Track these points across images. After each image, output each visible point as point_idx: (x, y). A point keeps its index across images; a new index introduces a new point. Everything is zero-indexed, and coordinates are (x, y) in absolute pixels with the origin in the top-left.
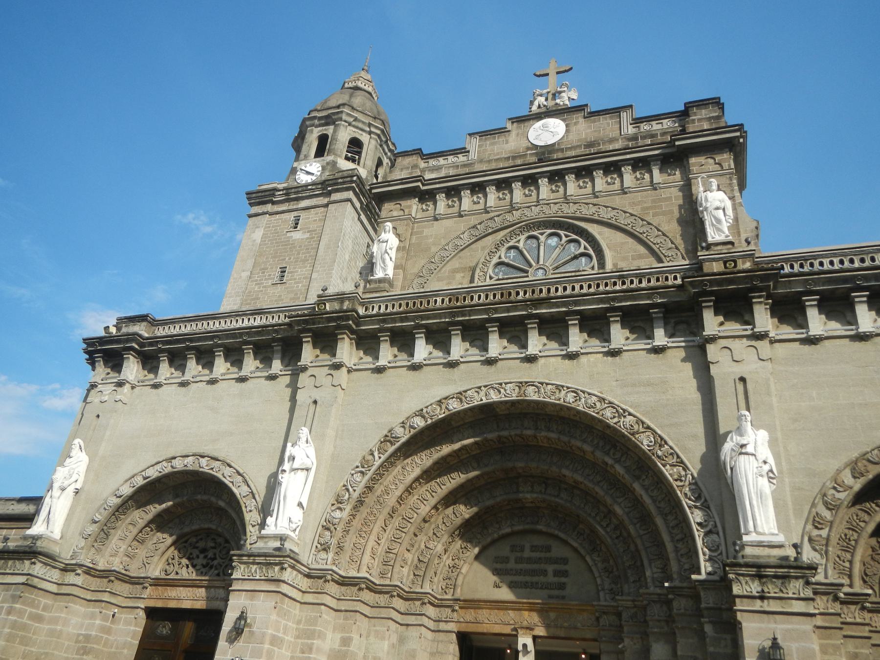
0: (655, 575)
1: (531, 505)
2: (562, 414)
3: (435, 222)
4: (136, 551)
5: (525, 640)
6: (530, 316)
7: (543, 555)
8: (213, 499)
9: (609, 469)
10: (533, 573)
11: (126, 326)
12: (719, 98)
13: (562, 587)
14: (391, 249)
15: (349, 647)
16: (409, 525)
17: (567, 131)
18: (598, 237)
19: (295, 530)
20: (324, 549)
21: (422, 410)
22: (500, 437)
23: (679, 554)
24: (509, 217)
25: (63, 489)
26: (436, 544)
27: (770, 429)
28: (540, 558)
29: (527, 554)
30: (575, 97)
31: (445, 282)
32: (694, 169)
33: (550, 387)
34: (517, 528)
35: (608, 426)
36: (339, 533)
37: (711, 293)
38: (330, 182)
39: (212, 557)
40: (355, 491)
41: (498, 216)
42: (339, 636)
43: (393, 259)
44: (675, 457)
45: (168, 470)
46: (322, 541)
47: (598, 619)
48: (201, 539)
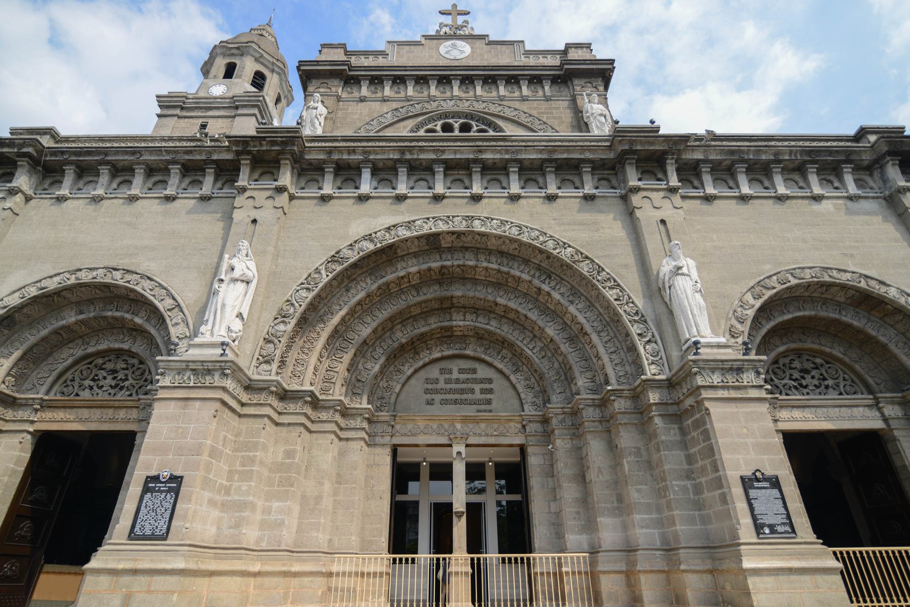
0: (586, 385)
1: (459, 333)
2: (504, 248)
4: (24, 371)
6: (476, 161)
7: (469, 376)
8: (128, 316)
9: (541, 298)
10: (462, 392)
13: (489, 402)
14: (320, 115)
15: (294, 458)
16: (351, 346)
17: (472, 52)
19: (234, 341)
20: (267, 362)
21: (371, 235)
22: (443, 267)
23: (614, 363)
26: (373, 365)
27: (692, 258)
28: (468, 379)
29: (455, 375)
33: (495, 221)
34: (446, 353)
35: (548, 257)
36: (281, 347)
37: (635, 152)
38: (238, 98)
39: (123, 378)
40: (300, 306)
41: (418, 104)
42: (281, 449)
43: (322, 125)
44: (612, 281)
45: (73, 280)
46: (264, 353)
47: (524, 427)
48: (110, 361)
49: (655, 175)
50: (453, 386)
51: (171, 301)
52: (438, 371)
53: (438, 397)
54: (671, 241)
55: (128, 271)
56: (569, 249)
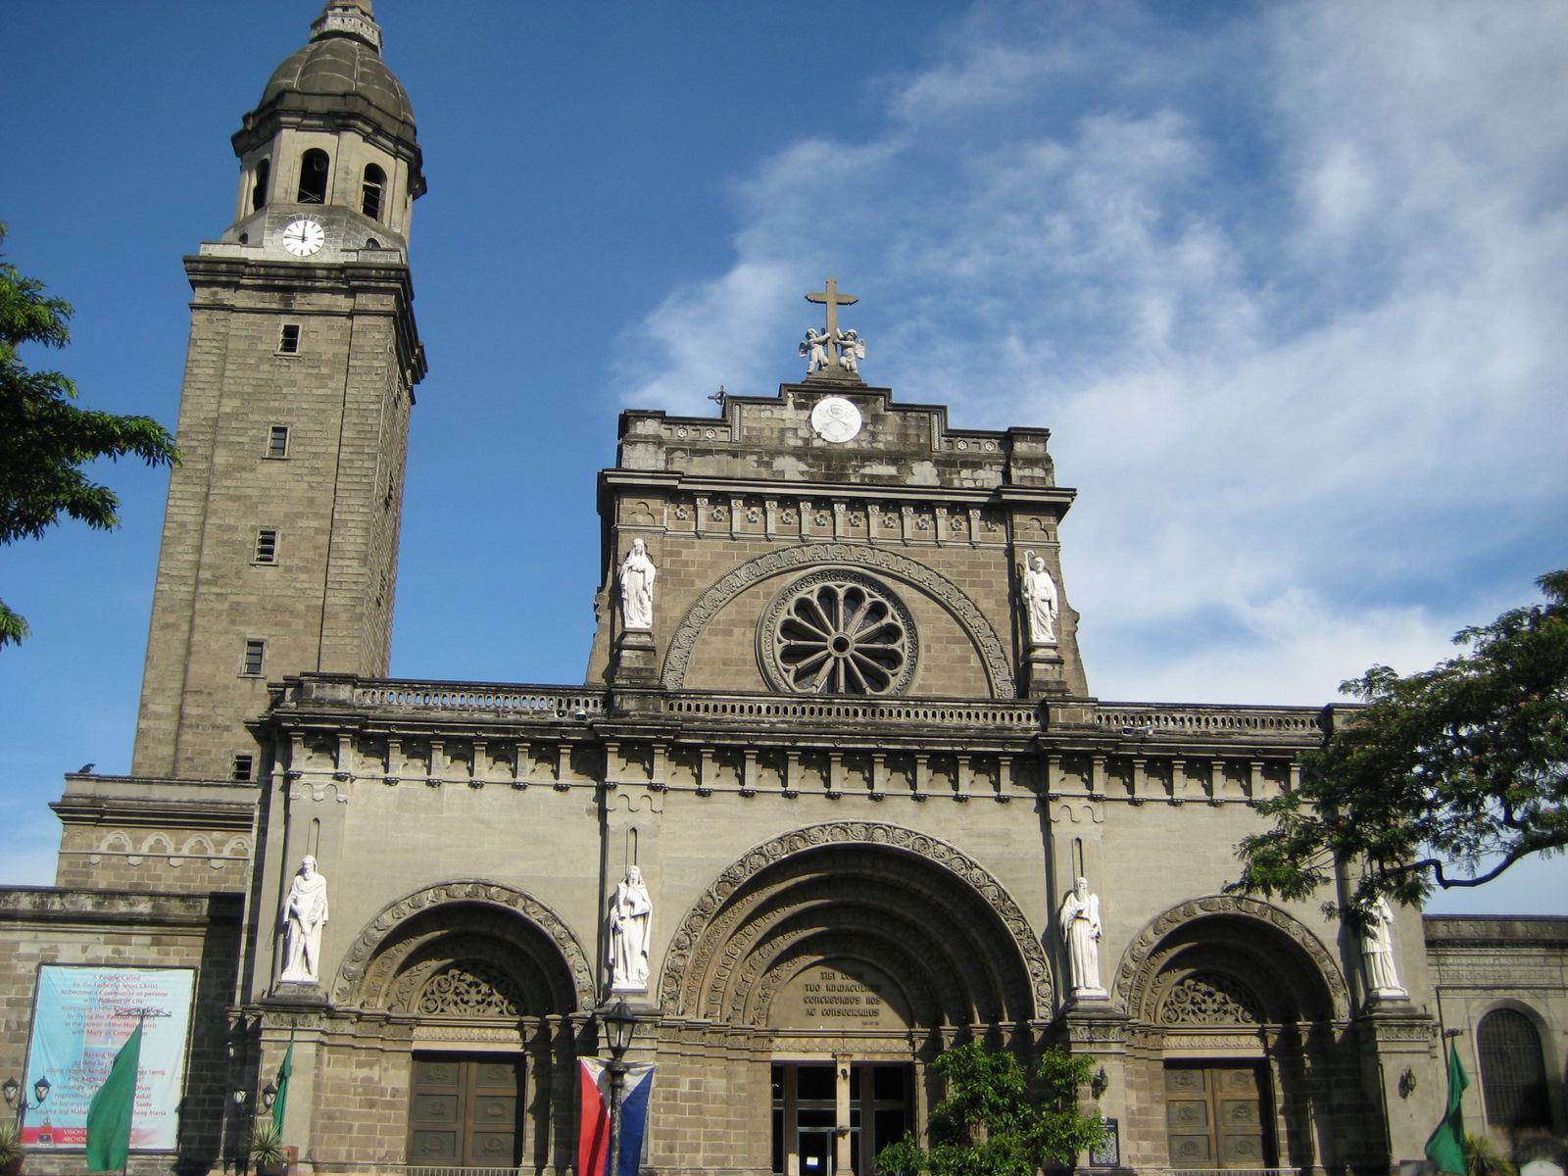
3: (697, 541)
5: (844, 1066)
8: (497, 932)
10: (846, 1001)
11: (318, 687)
12: (1048, 430)
13: (875, 1013)
16: (734, 961)
18: (910, 607)
24: (797, 554)
25: (314, 924)
30: (861, 355)
31: (719, 638)
32: (1018, 531)
38: (356, 272)
41: (784, 550)
45: (444, 899)
46: (668, 989)
49: (1082, 775)
50: (837, 994)
51: (559, 928)
52: (819, 975)
53: (819, 1007)
54: (1082, 875)
55: (503, 888)
56: (976, 870)
